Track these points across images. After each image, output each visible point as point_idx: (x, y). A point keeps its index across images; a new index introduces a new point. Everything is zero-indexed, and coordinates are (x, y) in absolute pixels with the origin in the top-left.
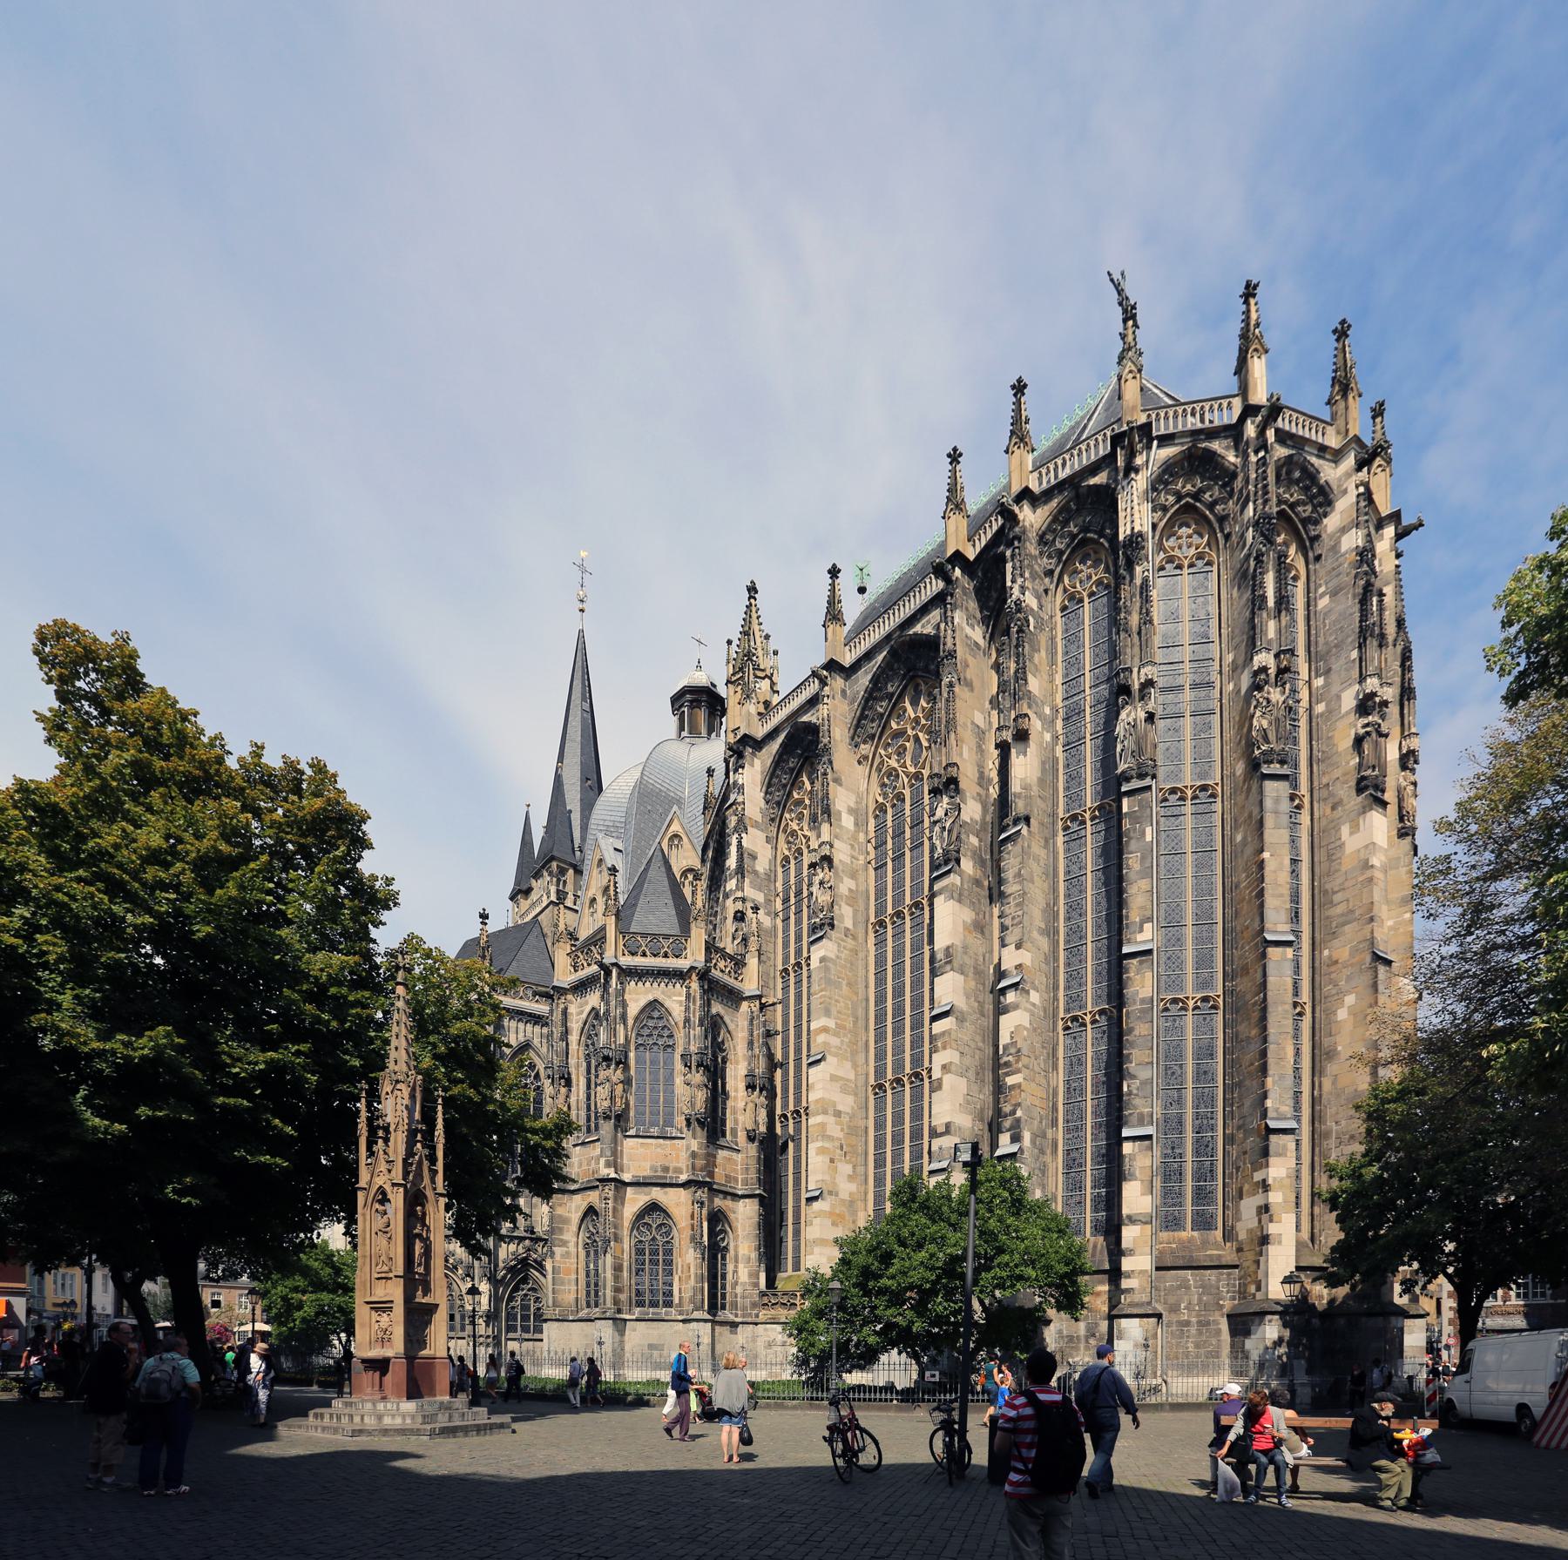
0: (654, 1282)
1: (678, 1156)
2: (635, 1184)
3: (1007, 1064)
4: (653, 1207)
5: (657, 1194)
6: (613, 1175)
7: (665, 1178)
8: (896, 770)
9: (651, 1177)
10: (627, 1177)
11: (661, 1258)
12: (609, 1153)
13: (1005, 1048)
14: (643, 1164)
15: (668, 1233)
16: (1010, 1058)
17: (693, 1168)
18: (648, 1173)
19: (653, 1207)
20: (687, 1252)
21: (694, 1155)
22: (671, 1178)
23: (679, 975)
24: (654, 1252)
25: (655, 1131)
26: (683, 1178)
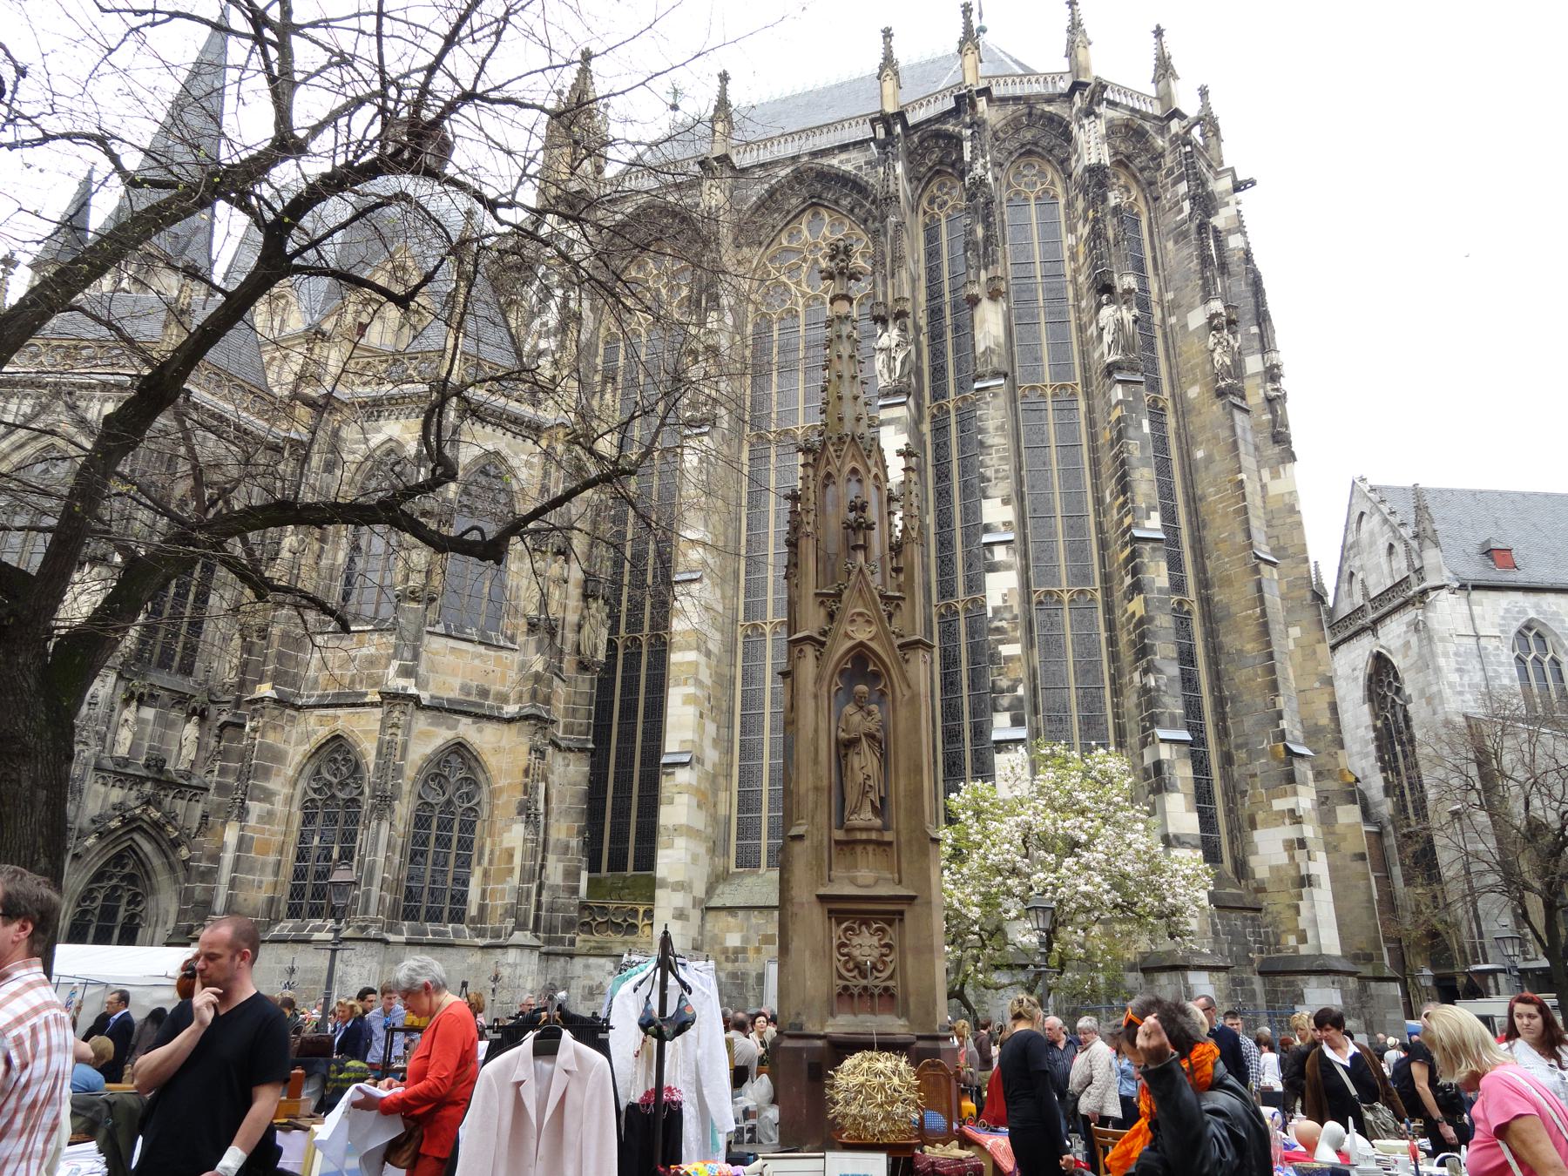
0: (439, 878)
1: (504, 675)
2: (444, 709)
3: (998, 630)
4: (459, 748)
5: (466, 729)
6: (412, 690)
7: (481, 706)
8: (785, 284)
9: (461, 702)
10: (425, 698)
11: (455, 835)
12: (407, 654)
13: (996, 610)
14: (450, 680)
15: (469, 797)
16: (1004, 624)
17: (534, 695)
18: (455, 694)
19: (459, 748)
20: (508, 828)
21: (537, 678)
22: (491, 707)
23: (535, 430)
24: (445, 825)
25: (472, 632)
26: (511, 709)
